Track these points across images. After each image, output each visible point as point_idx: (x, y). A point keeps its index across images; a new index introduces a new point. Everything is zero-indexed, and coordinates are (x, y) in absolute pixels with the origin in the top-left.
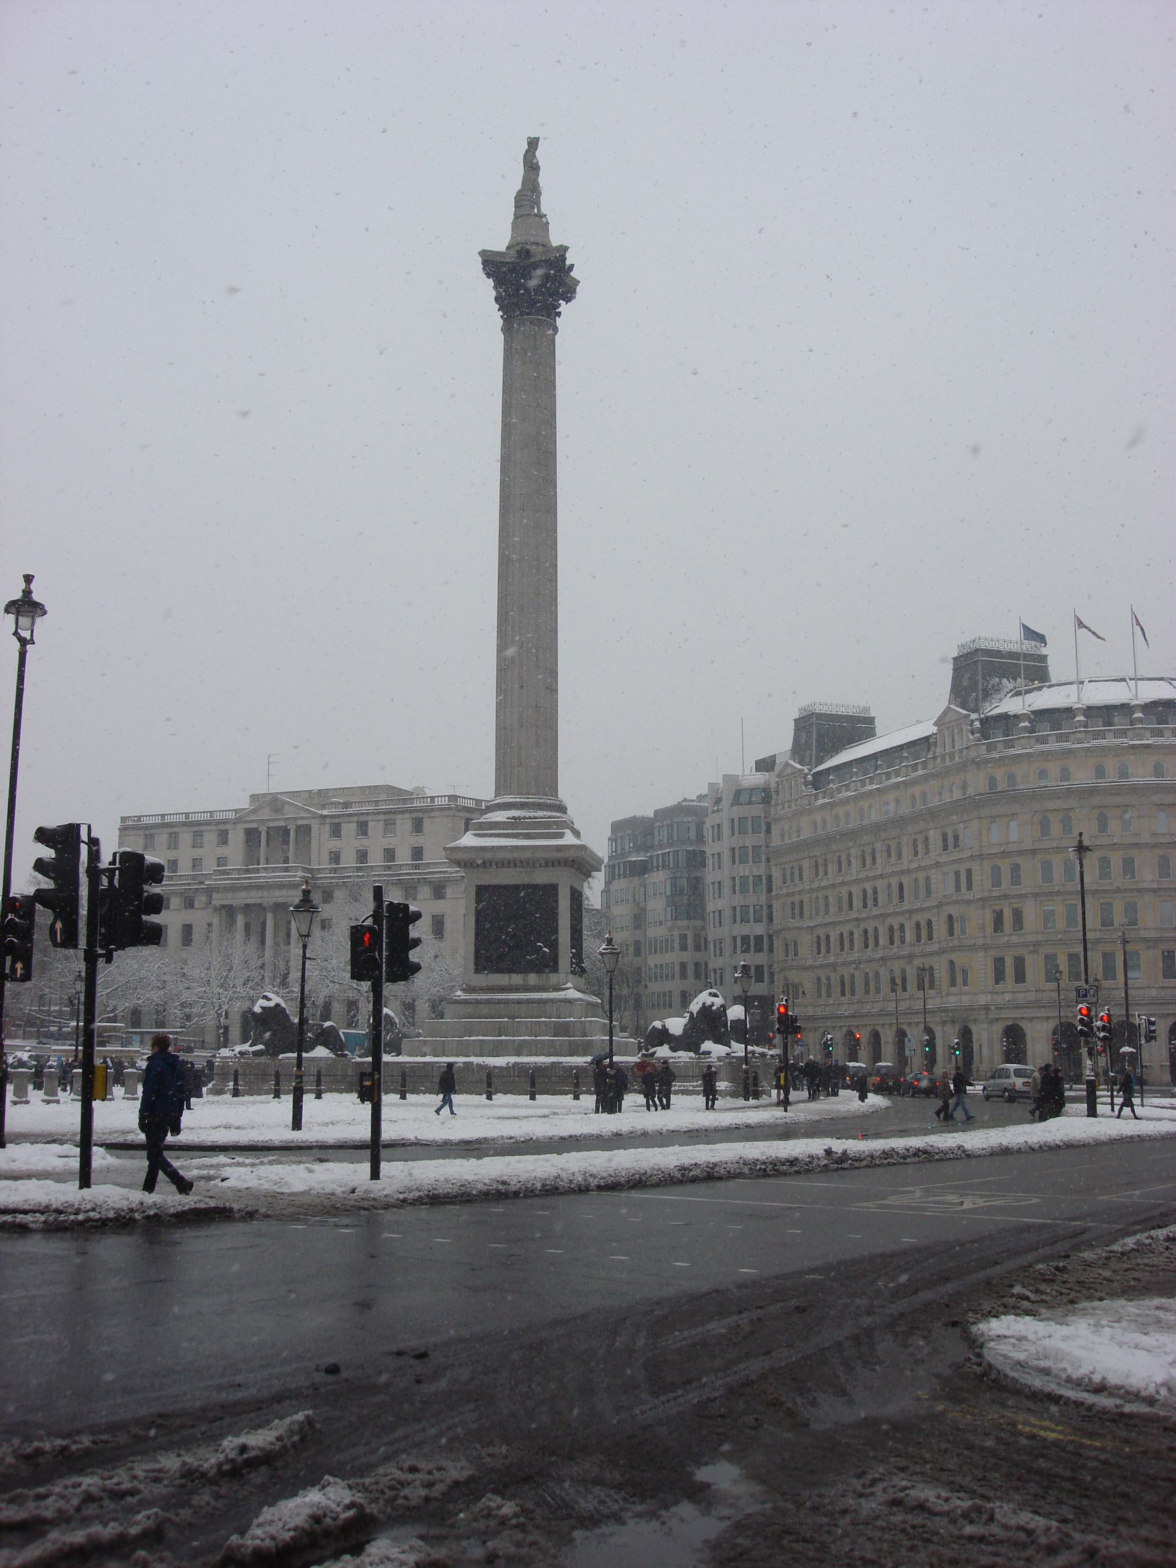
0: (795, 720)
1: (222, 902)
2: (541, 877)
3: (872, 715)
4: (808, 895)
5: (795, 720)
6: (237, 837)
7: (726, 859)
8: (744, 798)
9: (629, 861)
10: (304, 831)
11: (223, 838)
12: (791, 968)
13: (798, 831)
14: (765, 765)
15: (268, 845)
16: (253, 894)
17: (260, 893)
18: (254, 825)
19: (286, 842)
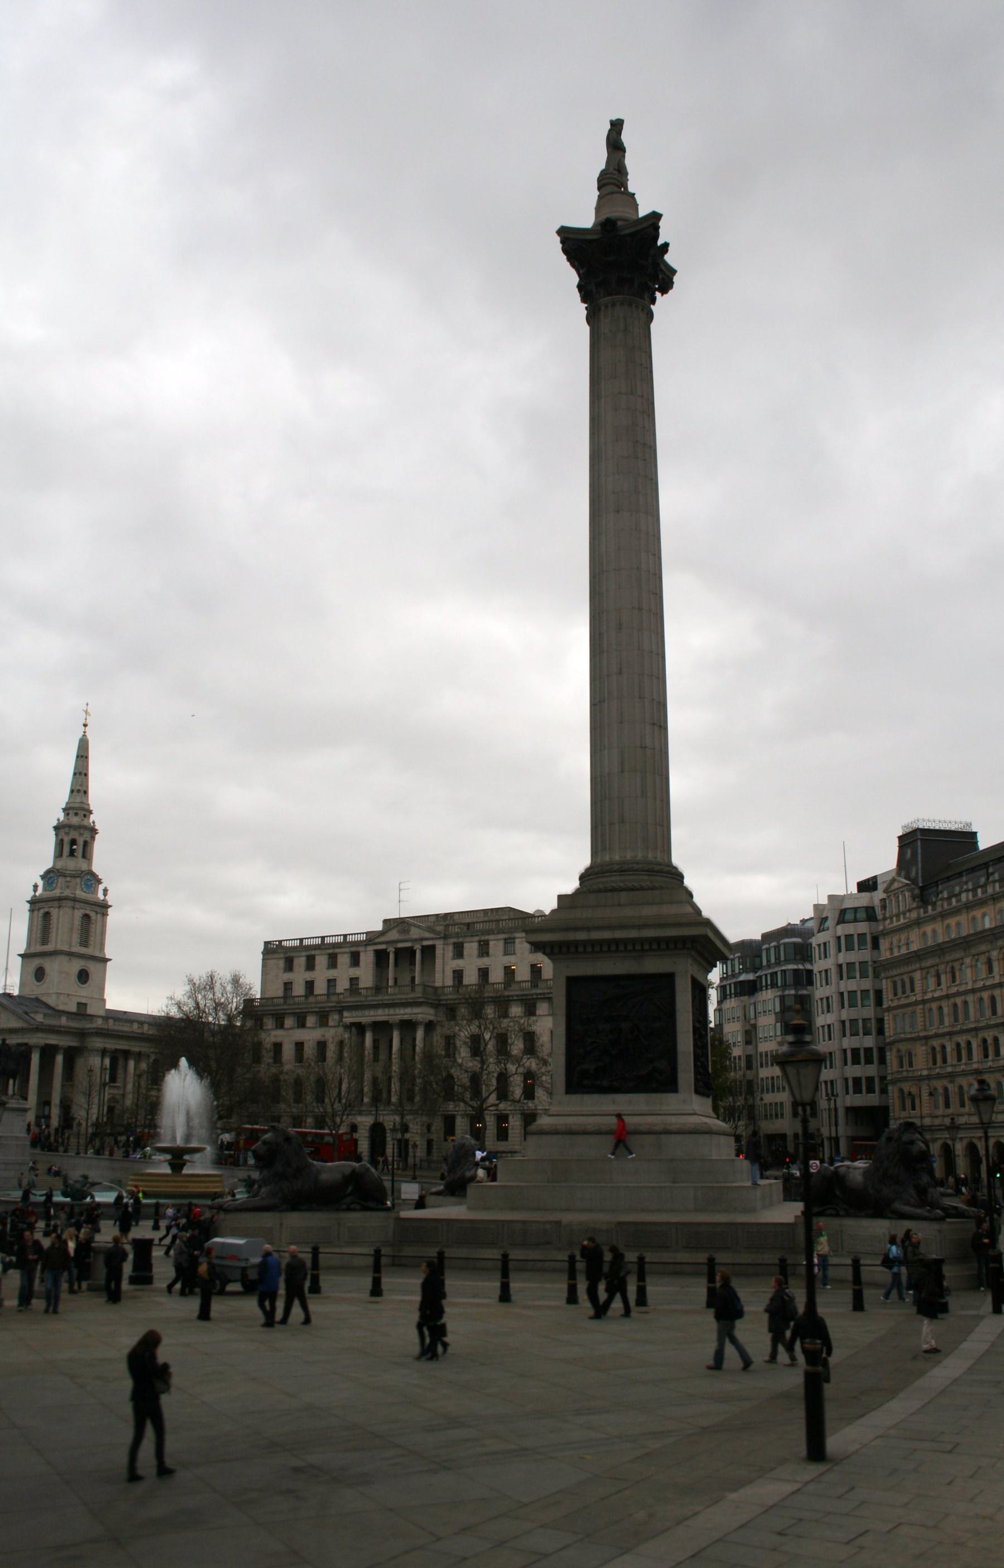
0: (900, 838)
1: (352, 1020)
2: (653, 965)
3: (974, 830)
4: (921, 1007)
5: (900, 838)
6: (367, 958)
7: (834, 976)
8: (849, 916)
9: (740, 982)
10: (429, 952)
11: (355, 960)
12: (905, 1079)
13: (907, 944)
14: (866, 886)
15: (396, 965)
16: (380, 1012)
17: (386, 1011)
18: (383, 947)
19: (413, 963)
